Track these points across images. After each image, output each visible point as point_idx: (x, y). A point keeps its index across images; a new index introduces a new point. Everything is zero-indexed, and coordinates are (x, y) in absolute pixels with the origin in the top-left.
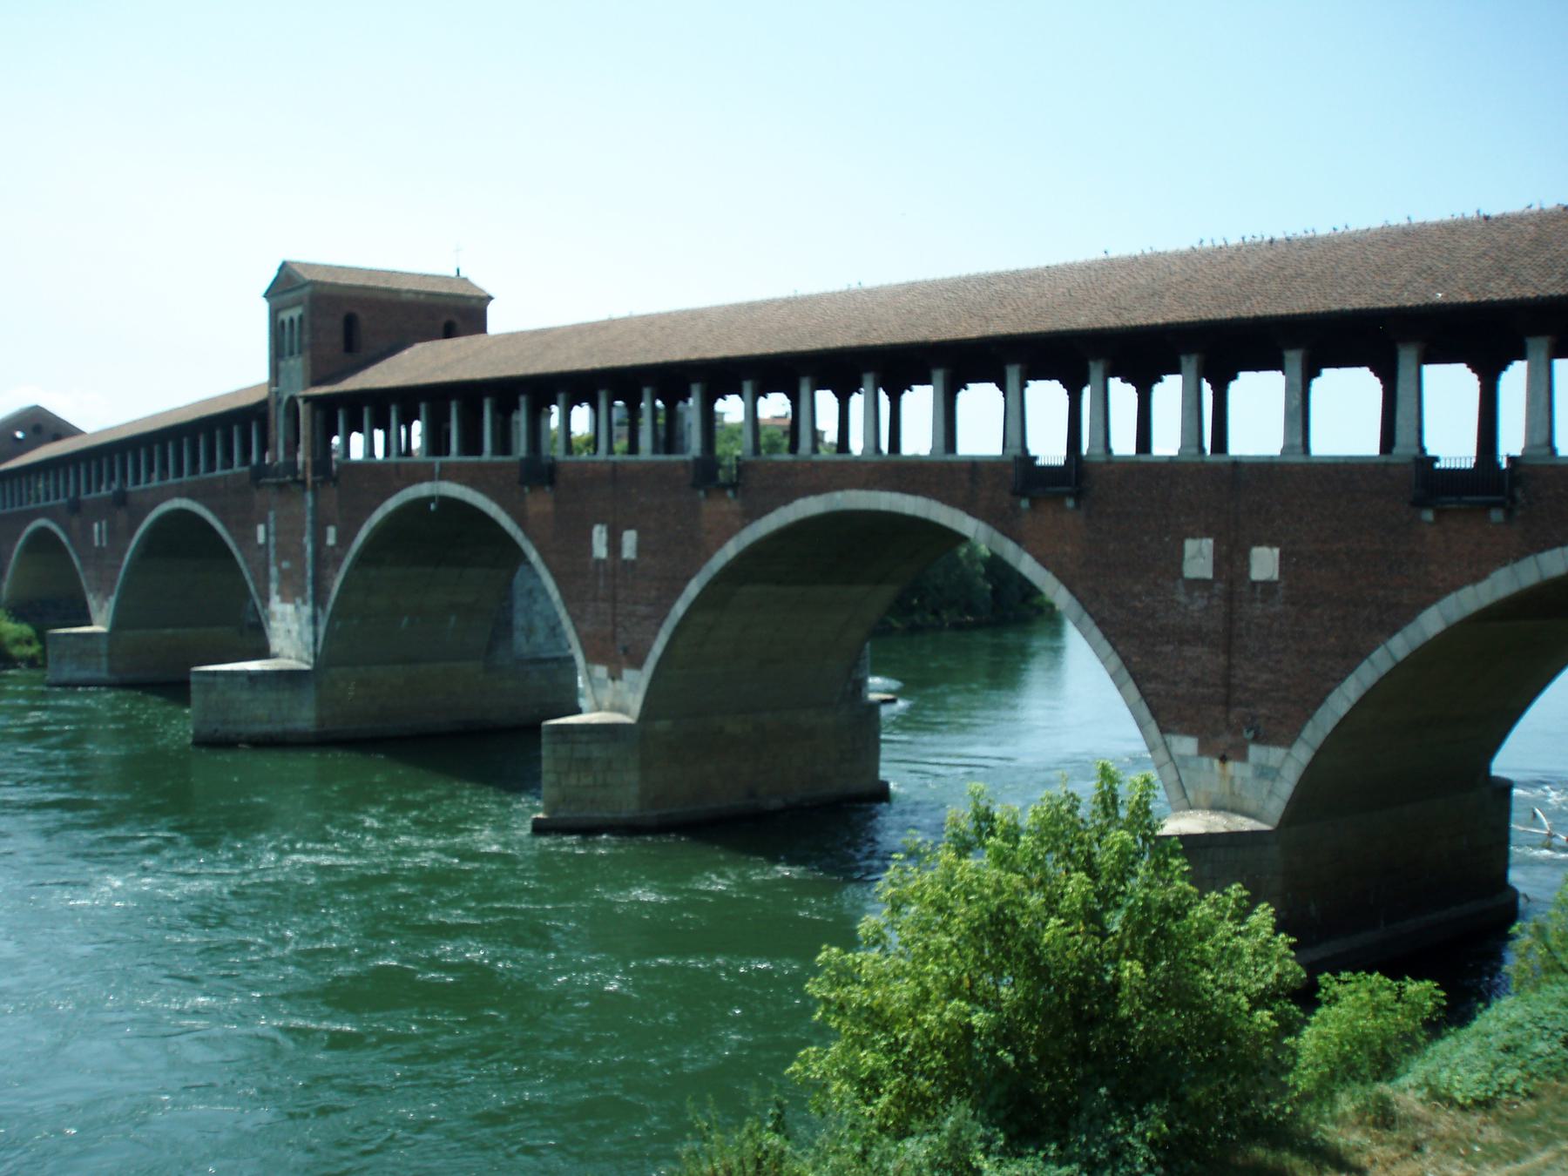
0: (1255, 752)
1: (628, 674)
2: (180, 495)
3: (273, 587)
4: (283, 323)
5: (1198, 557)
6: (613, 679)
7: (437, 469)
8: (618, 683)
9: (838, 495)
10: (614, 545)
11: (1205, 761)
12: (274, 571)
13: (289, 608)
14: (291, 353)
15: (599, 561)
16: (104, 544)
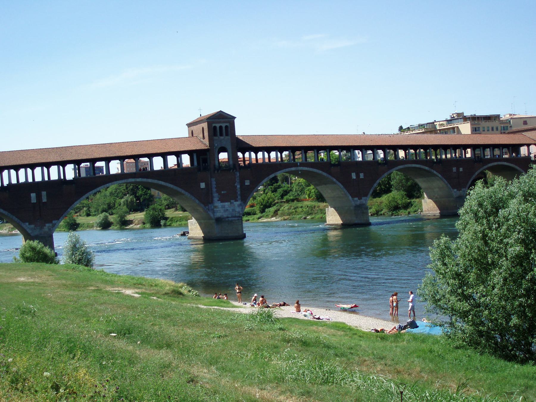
0: (462, 189)
1: (363, 198)
2: (134, 178)
3: (216, 199)
4: (215, 127)
5: (454, 169)
6: (360, 200)
7: (299, 164)
8: (361, 200)
9: (406, 165)
10: (358, 176)
11: (458, 192)
12: (216, 195)
13: (227, 204)
14: (221, 135)
15: (354, 179)
16: (44, 200)
